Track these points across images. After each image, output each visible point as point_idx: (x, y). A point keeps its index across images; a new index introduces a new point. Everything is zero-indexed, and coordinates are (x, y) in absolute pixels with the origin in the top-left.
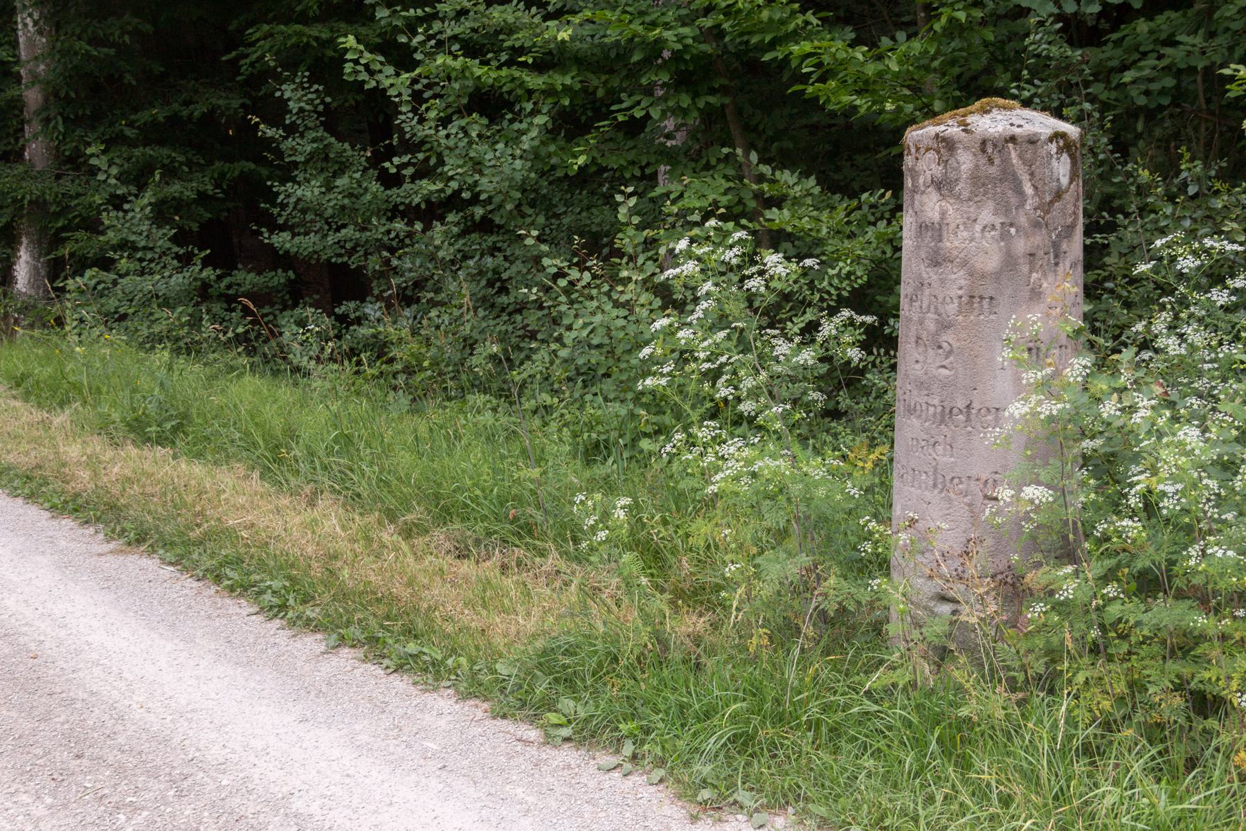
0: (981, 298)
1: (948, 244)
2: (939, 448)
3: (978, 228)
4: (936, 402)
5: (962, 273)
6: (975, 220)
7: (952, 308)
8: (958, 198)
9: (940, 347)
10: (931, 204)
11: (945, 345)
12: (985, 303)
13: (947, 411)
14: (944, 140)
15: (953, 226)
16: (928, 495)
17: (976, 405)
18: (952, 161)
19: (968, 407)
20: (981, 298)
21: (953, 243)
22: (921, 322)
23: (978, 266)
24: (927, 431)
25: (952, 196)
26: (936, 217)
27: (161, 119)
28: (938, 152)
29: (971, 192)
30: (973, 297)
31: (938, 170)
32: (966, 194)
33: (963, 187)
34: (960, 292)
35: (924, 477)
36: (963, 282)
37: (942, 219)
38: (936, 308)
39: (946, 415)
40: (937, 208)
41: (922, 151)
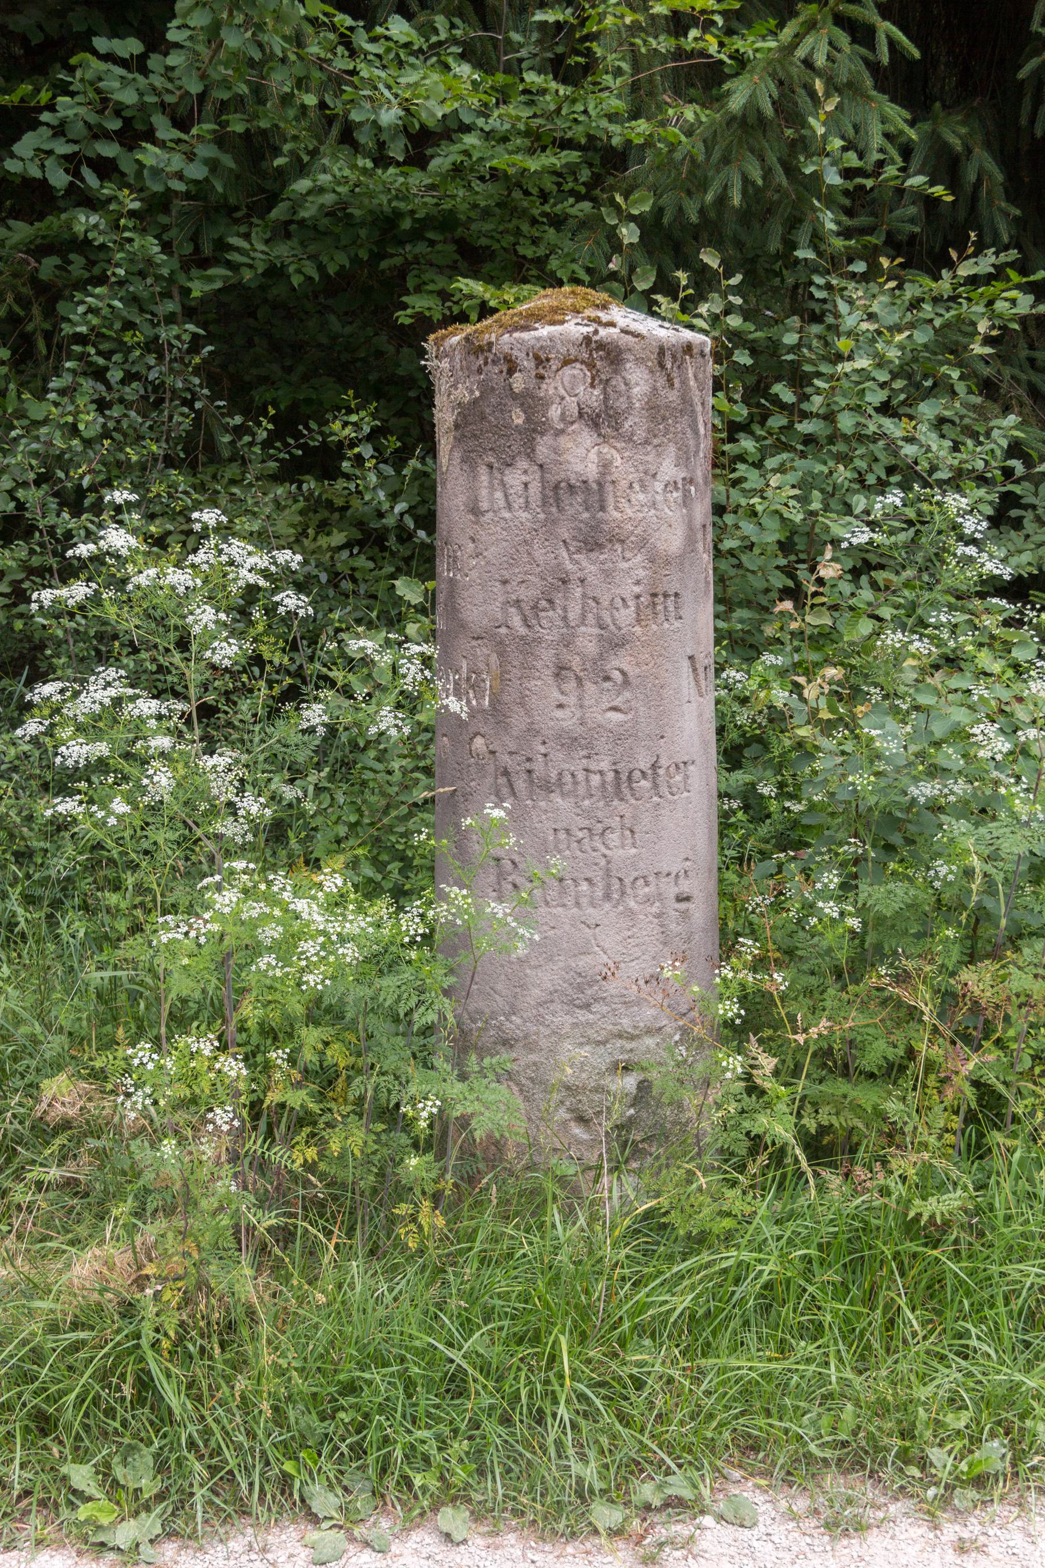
0: (666, 596)
1: (616, 515)
2: (613, 838)
3: (659, 486)
4: (605, 765)
5: (639, 558)
6: (654, 476)
7: (626, 616)
8: (630, 440)
9: (607, 678)
10: (581, 451)
11: (616, 675)
12: (670, 602)
13: (624, 777)
14: (601, 346)
15: (624, 484)
16: (593, 914)
17: (664, 762)
18: (617, 382)
19: (654, 766)
20: (666, 596)
21: (624, 511)
22: (567, 642)
23: (661, 546)
24: (587, 814)
25: (620, 437)
26: (592, 471)
27: (332, 880)
28: (591, 366)
29: (649, 431)
30: (654, 595)
31: (594, 397)
32: (640, 434)
33: (635, 423)
34: (637, 589)
35: (584, 887)
36: (642, 573)
37: (603, 474)
38: (599, 618)
39: (621, 783)
40: (593, 456)
41: (554, 365)
